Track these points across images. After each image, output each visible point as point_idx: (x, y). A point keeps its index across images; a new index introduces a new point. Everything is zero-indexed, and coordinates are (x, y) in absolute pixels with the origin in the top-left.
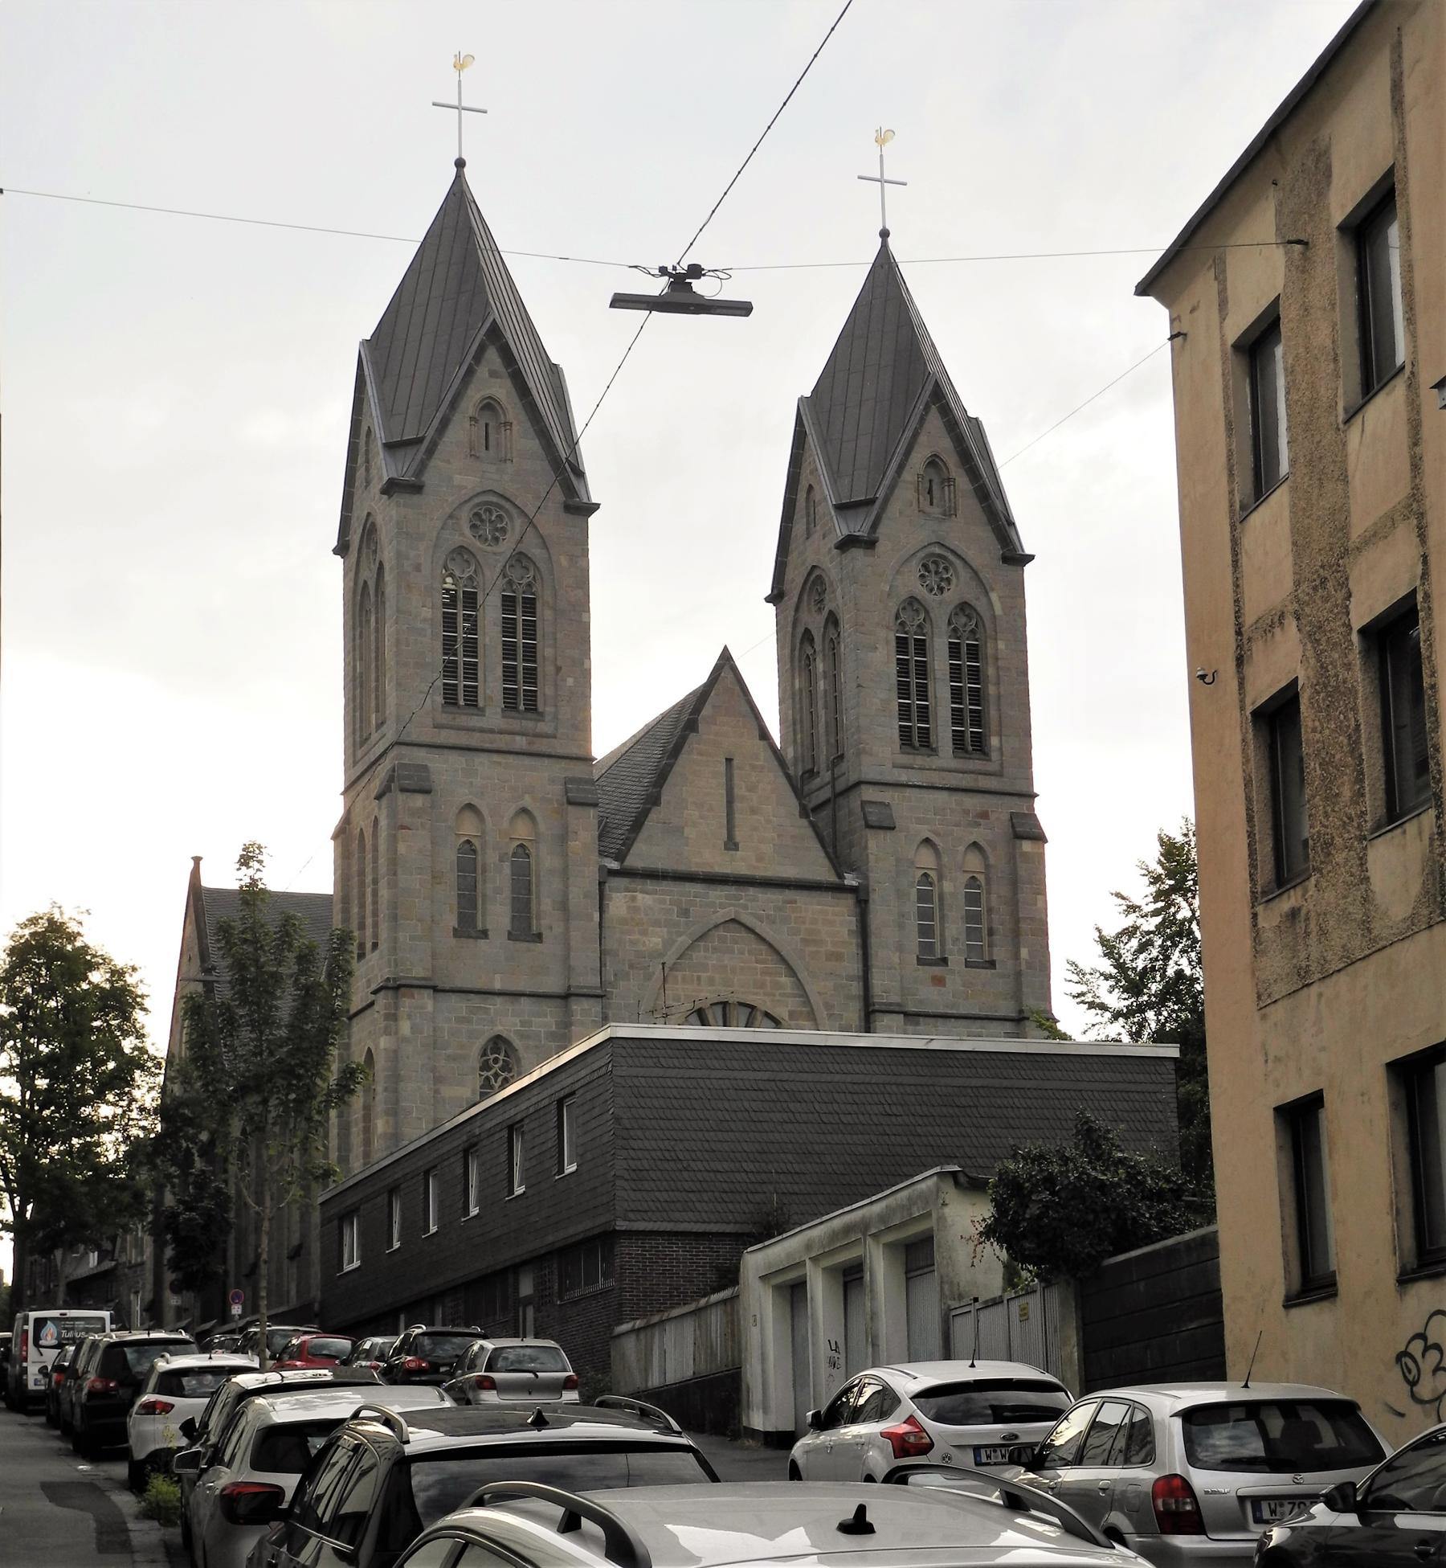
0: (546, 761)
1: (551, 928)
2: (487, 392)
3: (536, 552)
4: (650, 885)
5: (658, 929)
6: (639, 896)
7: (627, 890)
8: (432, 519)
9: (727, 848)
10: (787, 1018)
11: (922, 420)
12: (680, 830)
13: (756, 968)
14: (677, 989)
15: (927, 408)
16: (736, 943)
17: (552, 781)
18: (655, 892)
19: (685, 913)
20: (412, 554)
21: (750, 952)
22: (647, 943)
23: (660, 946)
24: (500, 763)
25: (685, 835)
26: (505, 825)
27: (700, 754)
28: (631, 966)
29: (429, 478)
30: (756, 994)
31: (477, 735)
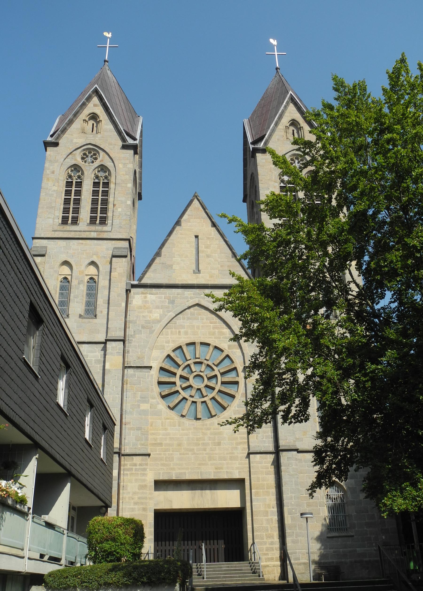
0: (105, 241)
1: (102, 312)
2: (91, 111)
3: (108, 164)
4: (154, 290)
5: (158, 310)
6: (149, 296)
7: (143, 293)
8: (61, 155)
9: (194, 272)
10: (227, 349)
11: (286, 107)
12: (171, 266)
13: (210, 326)
14: (168, 338)
15: (287, 103)
16: (200, 315)
17: (107, 249)
18: (157, 294)
19: (172, 302)
20: (51, 167)
21: (207, 319)
22: (152, 316)
23: (158, 318)
24: (82, 244)
25: (173, 268)
26: (83, 267)
27: (181, 234)
28: (143, 327)
29: (61, 142)
30: (210, 338)
31: (73, 233)
